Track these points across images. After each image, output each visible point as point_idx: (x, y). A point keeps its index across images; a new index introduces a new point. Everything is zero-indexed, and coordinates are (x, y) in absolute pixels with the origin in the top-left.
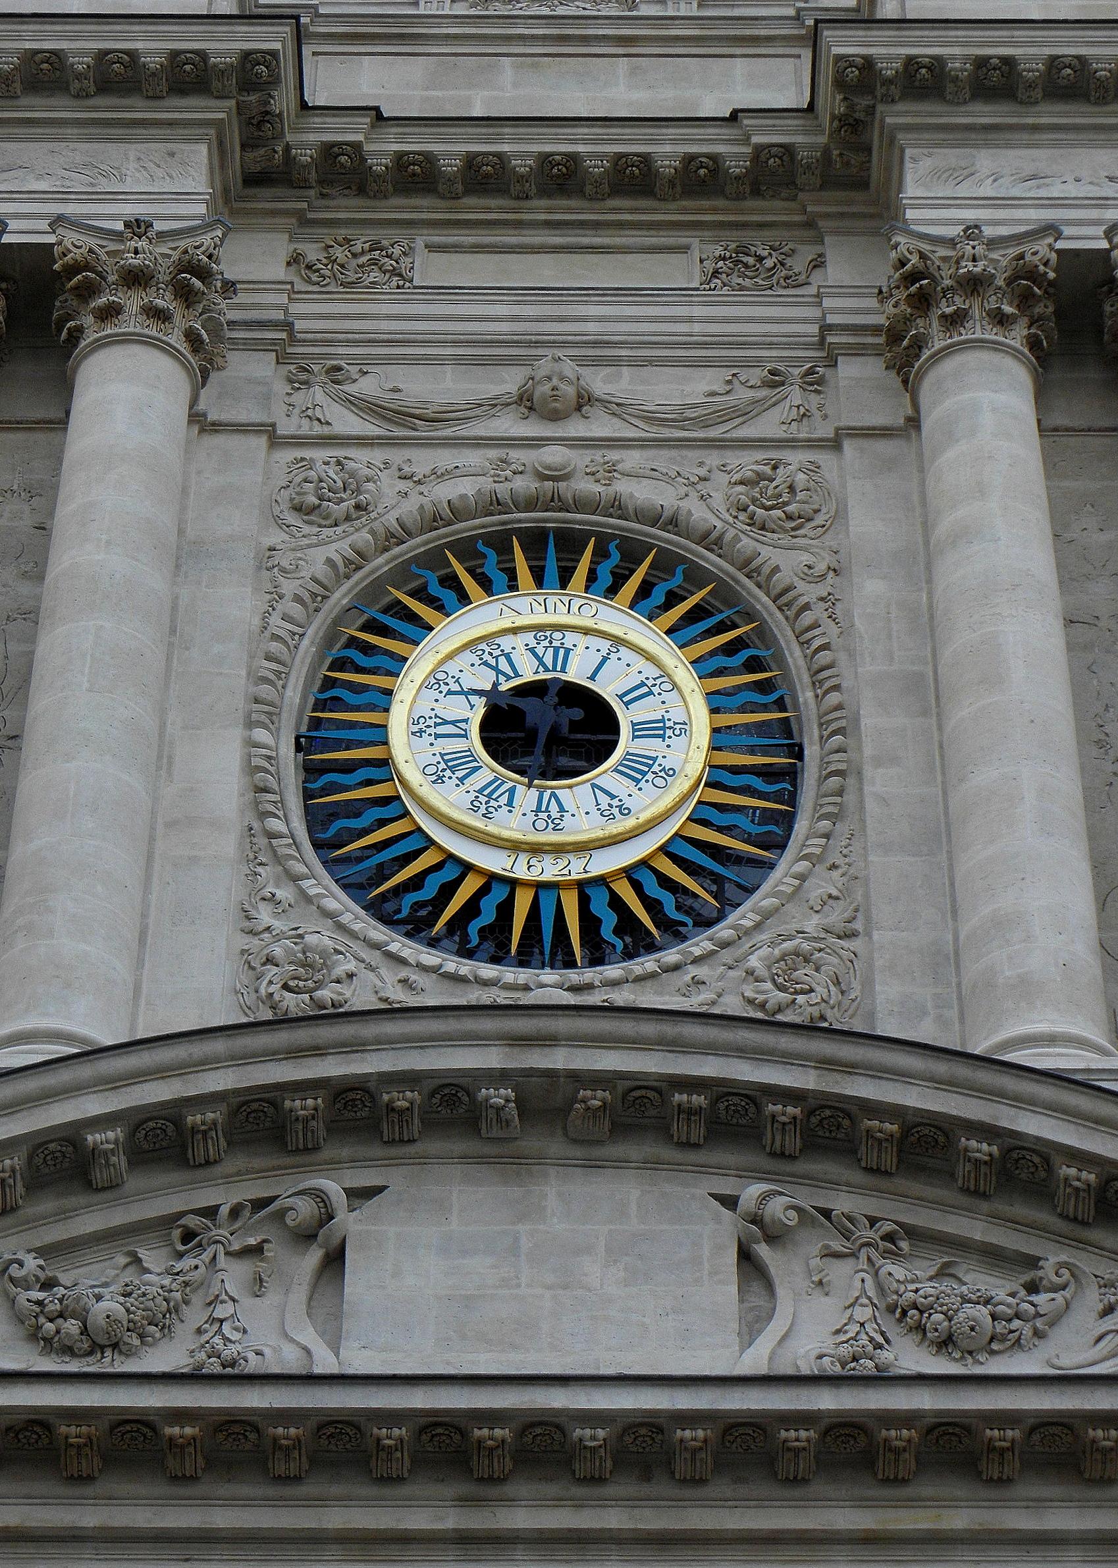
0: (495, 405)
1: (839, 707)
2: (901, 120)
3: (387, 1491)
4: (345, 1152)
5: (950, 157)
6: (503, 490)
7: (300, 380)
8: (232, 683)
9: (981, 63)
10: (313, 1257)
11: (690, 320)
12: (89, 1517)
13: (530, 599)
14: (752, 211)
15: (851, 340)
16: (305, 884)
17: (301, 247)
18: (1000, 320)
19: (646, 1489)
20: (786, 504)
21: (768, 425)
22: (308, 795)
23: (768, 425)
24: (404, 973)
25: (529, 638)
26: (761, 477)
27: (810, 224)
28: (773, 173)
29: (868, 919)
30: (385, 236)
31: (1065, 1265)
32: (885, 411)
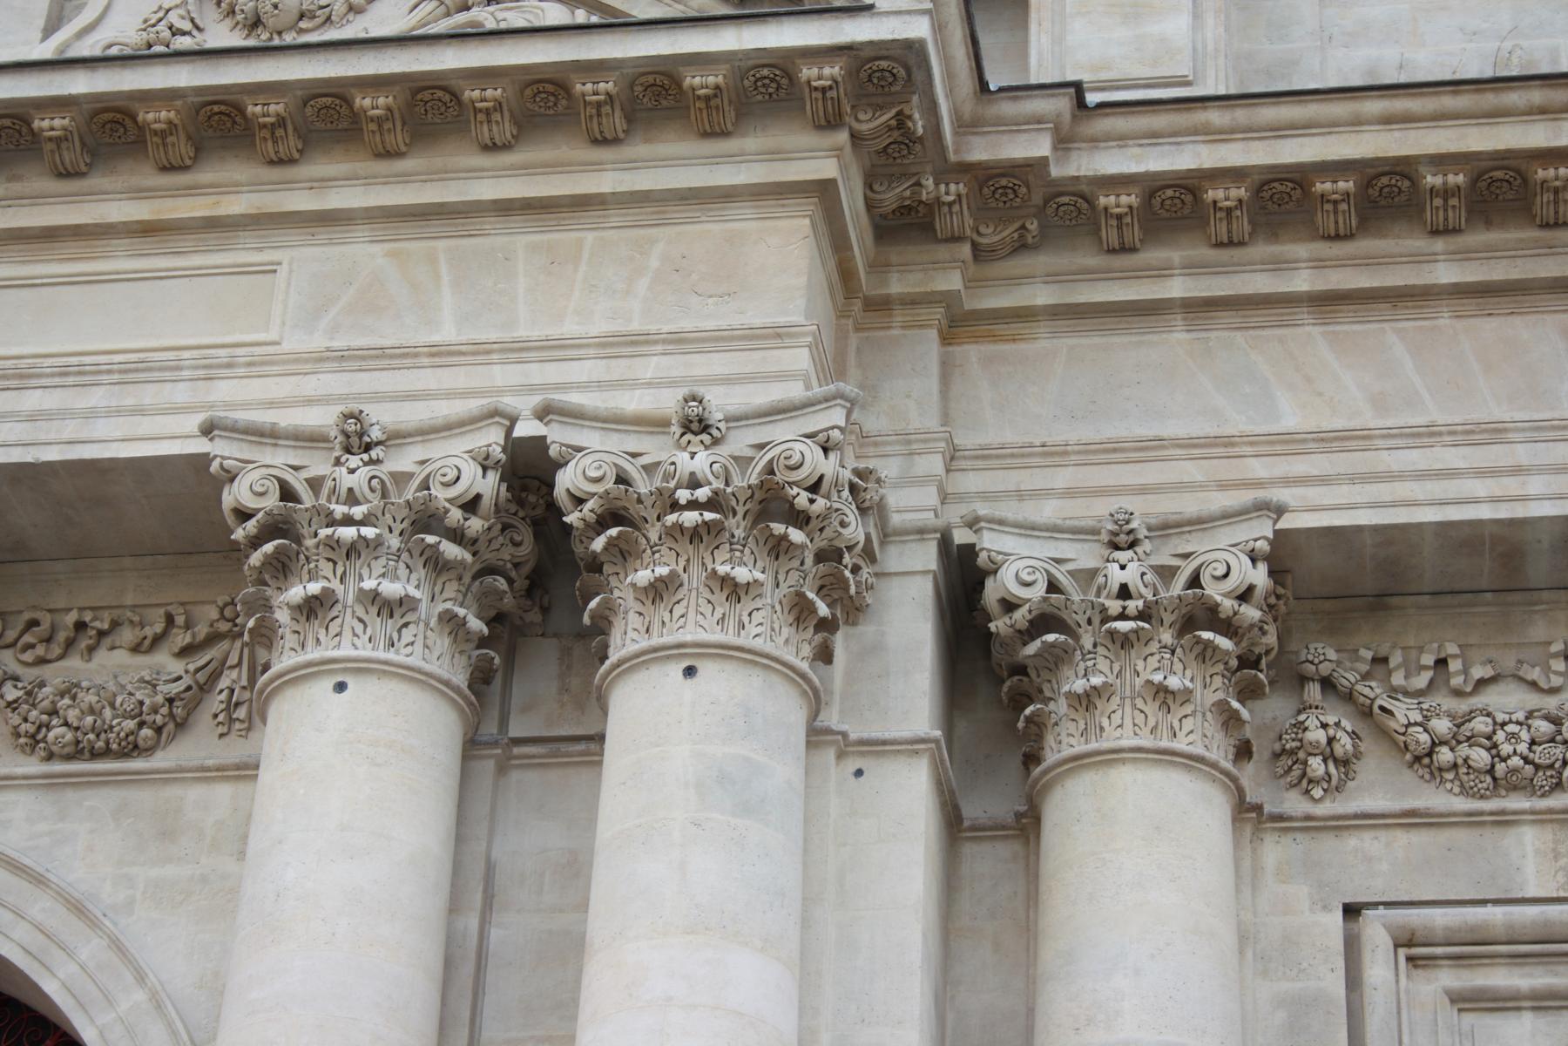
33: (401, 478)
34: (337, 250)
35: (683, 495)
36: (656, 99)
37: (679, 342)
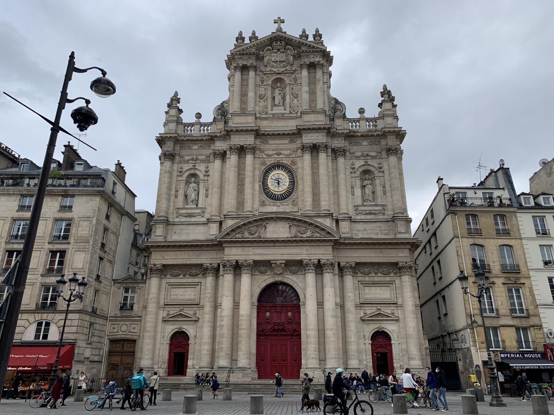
0: (274, 154)
8: (257, 179)
21: (293, 156)
23: (293, 156)
28: (294, 134)
32: (301, 155)
36: (325, 241)
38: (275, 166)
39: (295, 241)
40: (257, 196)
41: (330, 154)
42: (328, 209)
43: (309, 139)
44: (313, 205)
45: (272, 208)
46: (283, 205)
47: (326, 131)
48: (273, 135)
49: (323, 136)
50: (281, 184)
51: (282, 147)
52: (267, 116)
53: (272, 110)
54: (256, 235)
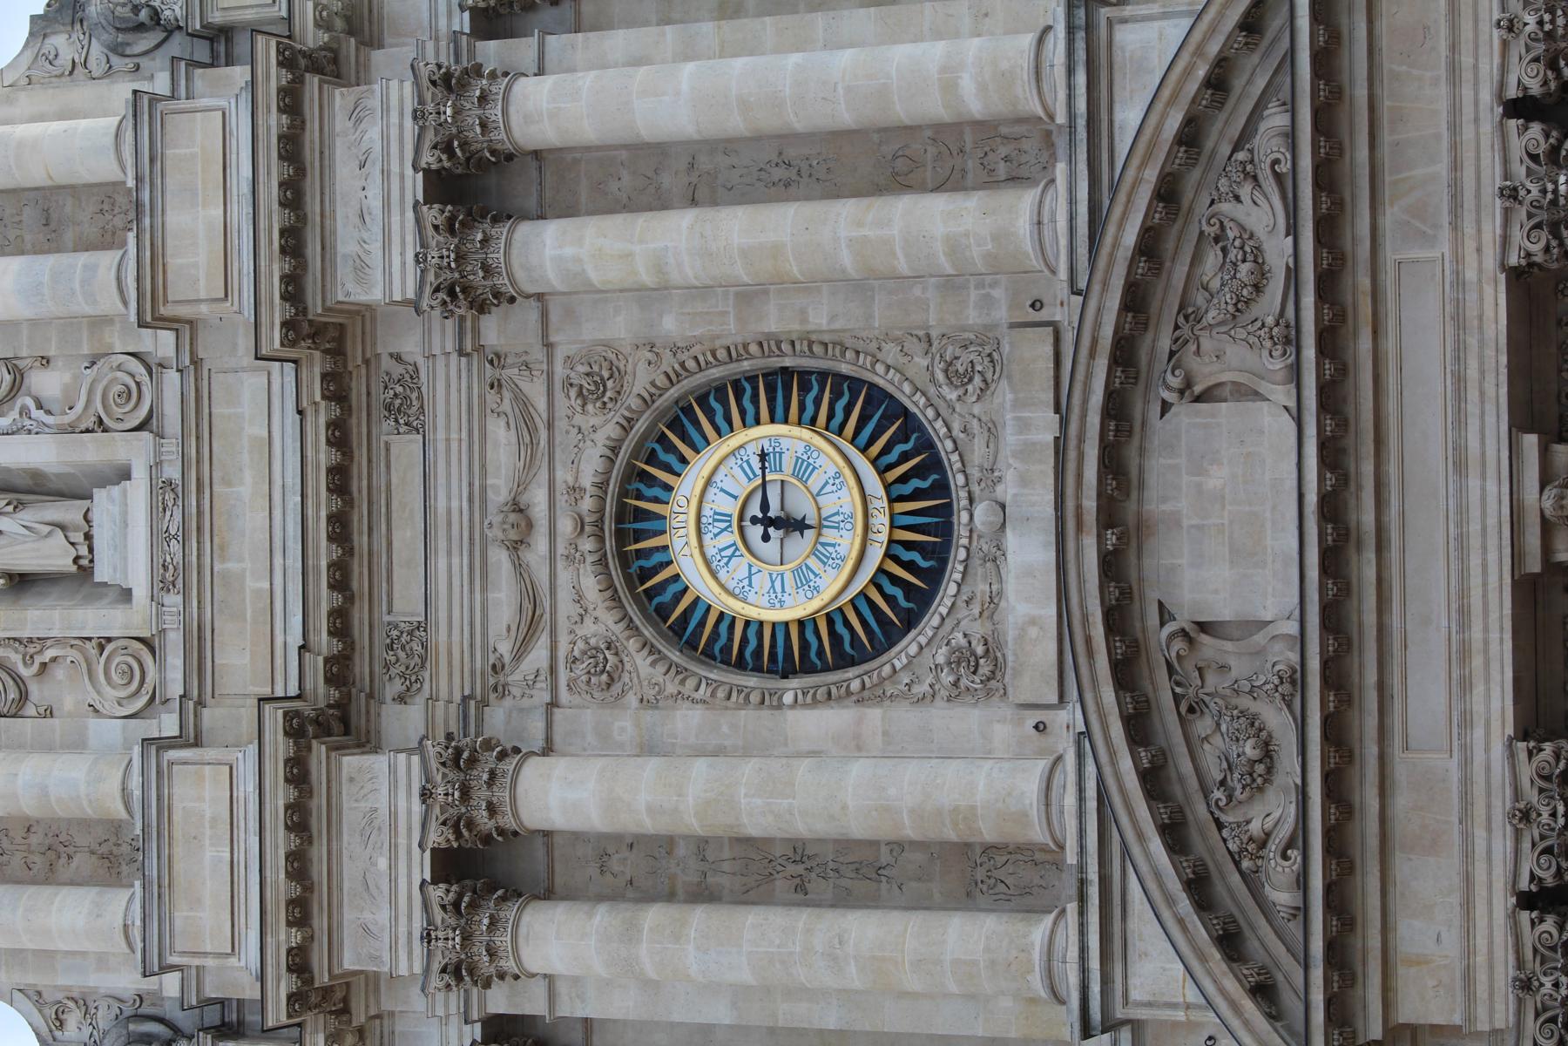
0: (519, 567)
1: (761, 344)
2: (319, 303)
3: (1355, 589)
4: (1138, 625)
5: (344, 273)
6: (590, 559)
7: (501, 690)
8: (750, 719)
9: (283, 251)
10: (1204, 638)
11: (448, 440)
12: (1372, 750)
13: (675, 538)
14: (359, 400)
15: (469, 336)
16: (898, 665)
17: (388, 698)
18: (485, 241)
19: (1352, 451)
20: (602, 378)
22: (826, 669)
24: (961, 603)
25: (707, 538)
26: (580, 394)
27: (367, 362)
28: (337, 389)
29: (919, 328)
30: (381, 640)
31: (1208, 223)
33: (1529, 172)
34: (1388, 234)
35: (1547, 27)
36: (1325, 61)
37: (1454, 48)
38: (624, 560)
39: (1331, 341)
40: (905, 717)
41: (522, 50)
42: (1027, 40)
43: (378, 243)
44: (990, 182)
45: (1020, 574)
46: (991, 476)
47: (313, 82)
48: (340, 579)
49: (357, 114)
50: (801, 506)
51: (450, 498)
52: (174, 639)
53: (126, 595)
54: (1277, 720)
